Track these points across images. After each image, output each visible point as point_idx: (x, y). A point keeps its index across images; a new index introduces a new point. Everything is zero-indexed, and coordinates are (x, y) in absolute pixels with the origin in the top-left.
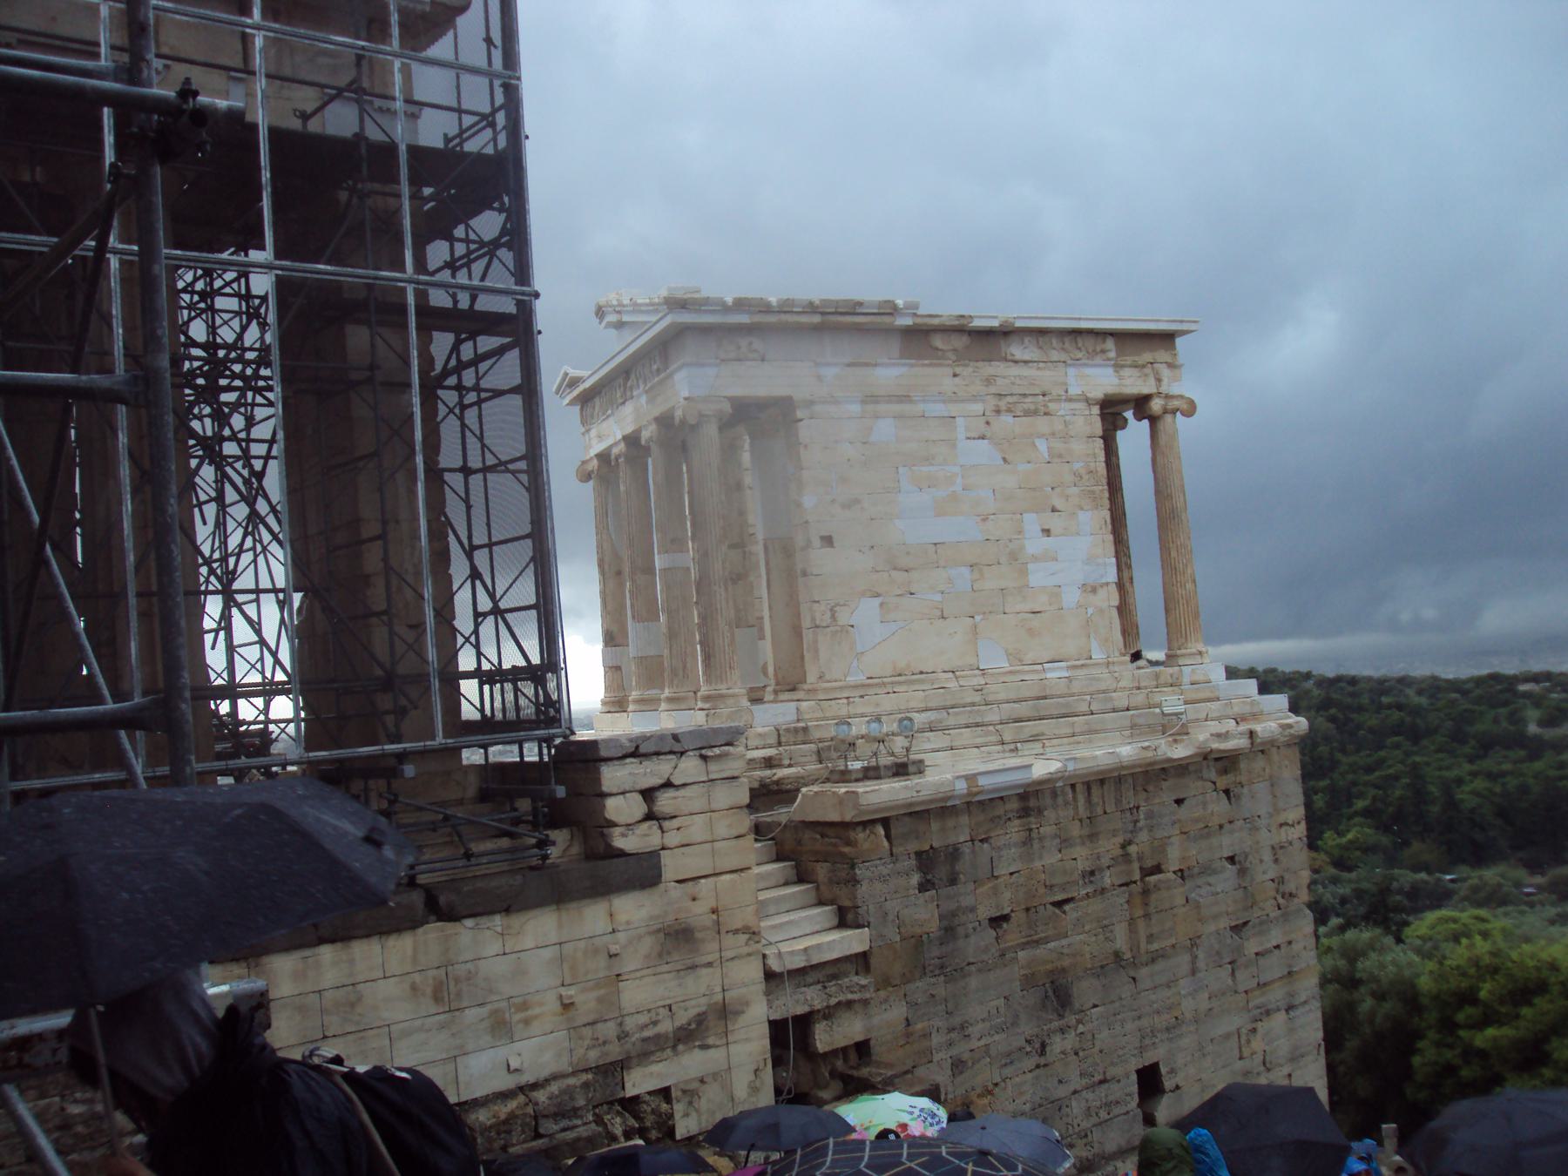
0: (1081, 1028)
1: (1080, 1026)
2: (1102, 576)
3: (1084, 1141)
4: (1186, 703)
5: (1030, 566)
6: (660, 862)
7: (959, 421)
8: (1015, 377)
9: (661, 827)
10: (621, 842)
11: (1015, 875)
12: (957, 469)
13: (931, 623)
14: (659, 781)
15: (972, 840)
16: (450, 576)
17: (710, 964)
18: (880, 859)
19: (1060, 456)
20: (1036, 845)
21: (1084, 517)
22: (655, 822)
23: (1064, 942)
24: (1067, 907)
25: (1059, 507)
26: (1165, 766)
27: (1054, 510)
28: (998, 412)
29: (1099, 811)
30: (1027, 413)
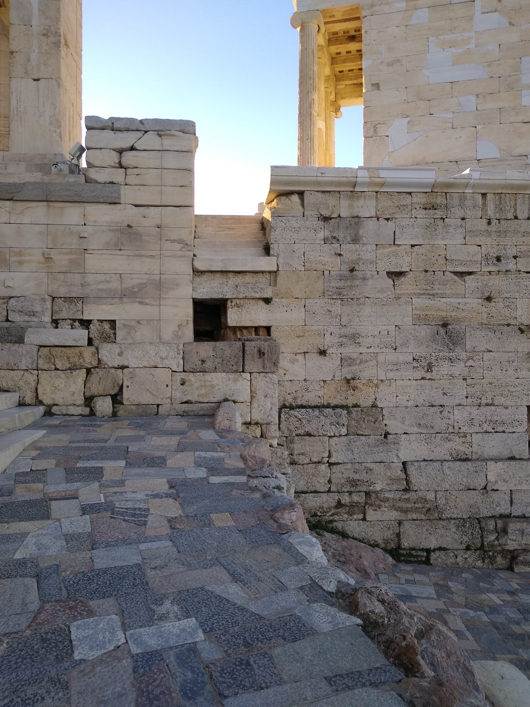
0: (470, 363)
1: (471, 361)
3: (463, 439)
17: (153, 256)
18: (293, 217)
22: (124, 170)
23: (460, 300)
24: (467, 278)
29: (510, 216)
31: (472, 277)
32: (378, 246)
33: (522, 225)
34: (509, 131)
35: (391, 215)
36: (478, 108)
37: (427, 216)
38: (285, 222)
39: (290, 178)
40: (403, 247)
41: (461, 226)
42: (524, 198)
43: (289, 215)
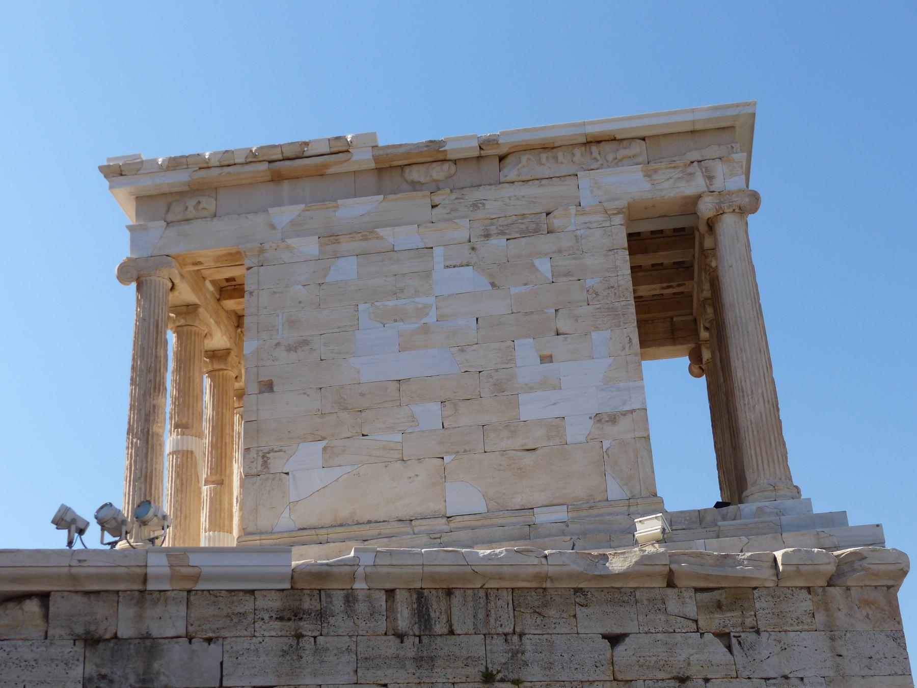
5: (522, 397)
7: (438, 252)
12: (431, 300)
13: (386, 467)
18: (25, 639)
19: (568, 274)
20: (307, 657)
21: (595, 336)
25: (562, 329)
27: (558, 335)
28: (487, 236)
30: (526, 233)
33: (463, 645)
34: (500, 465)
35: (214, 632)
37: (283, 633)
38: (8, 649)
39: (19, 571)
41: (348, 650)
42: (465, 597)
43: (18, 637)
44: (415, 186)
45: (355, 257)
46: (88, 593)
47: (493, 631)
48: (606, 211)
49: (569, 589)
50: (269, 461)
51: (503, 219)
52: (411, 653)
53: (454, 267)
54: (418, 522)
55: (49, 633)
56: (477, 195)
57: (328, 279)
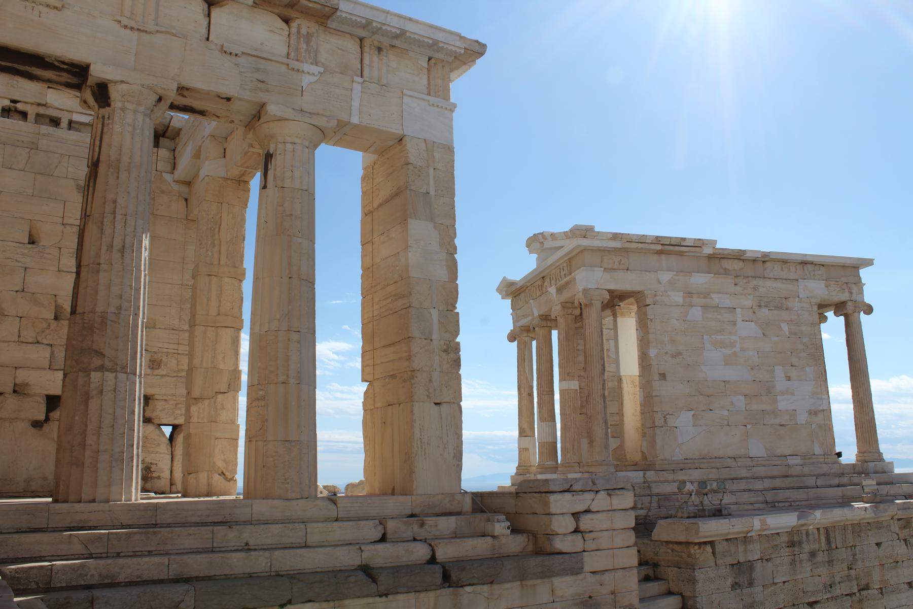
2: (820, 406)
4: (878, 484)
5: (779, 397)
6: (582, 559)
8: (769, 287)
9: (583, 538)
10: (561, 544)
11: (786, 583)
13: (722, 428)
14: (582, 508)
15: (762, 559)
16: (460, 375)
18: (709, 567)
19: (795, 334)
20: (798, 565)
21: (808, 369)
22: (580, 534)
24: (815, 606)
25: (794, 364)
26: (870, 521)
27: (792, 366)
28: (760, 306)
31: (819, 606)
32: (764, 588)
36: (747, 408)
37: (790, 554)
40: (778, 586)
42: (839, 529)
44: (726, 272)
45: (700, 308)
46: (727, 540)
47: (848, 546)
48: (810, 303)
49: (866, 523)
50: (667, 420)
51: (766, 298)
52: (826, 559)
53: (746, 321)
54: (740, 460)
55: (718, 562)
56: (755, 282)
57: (688, 318)
